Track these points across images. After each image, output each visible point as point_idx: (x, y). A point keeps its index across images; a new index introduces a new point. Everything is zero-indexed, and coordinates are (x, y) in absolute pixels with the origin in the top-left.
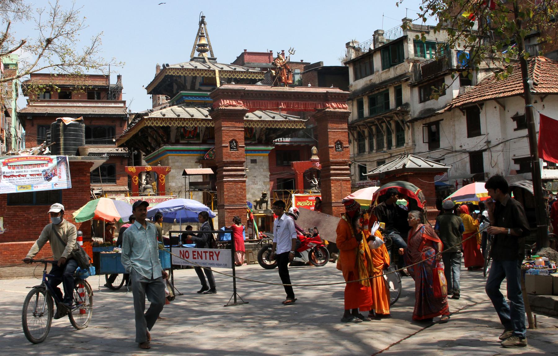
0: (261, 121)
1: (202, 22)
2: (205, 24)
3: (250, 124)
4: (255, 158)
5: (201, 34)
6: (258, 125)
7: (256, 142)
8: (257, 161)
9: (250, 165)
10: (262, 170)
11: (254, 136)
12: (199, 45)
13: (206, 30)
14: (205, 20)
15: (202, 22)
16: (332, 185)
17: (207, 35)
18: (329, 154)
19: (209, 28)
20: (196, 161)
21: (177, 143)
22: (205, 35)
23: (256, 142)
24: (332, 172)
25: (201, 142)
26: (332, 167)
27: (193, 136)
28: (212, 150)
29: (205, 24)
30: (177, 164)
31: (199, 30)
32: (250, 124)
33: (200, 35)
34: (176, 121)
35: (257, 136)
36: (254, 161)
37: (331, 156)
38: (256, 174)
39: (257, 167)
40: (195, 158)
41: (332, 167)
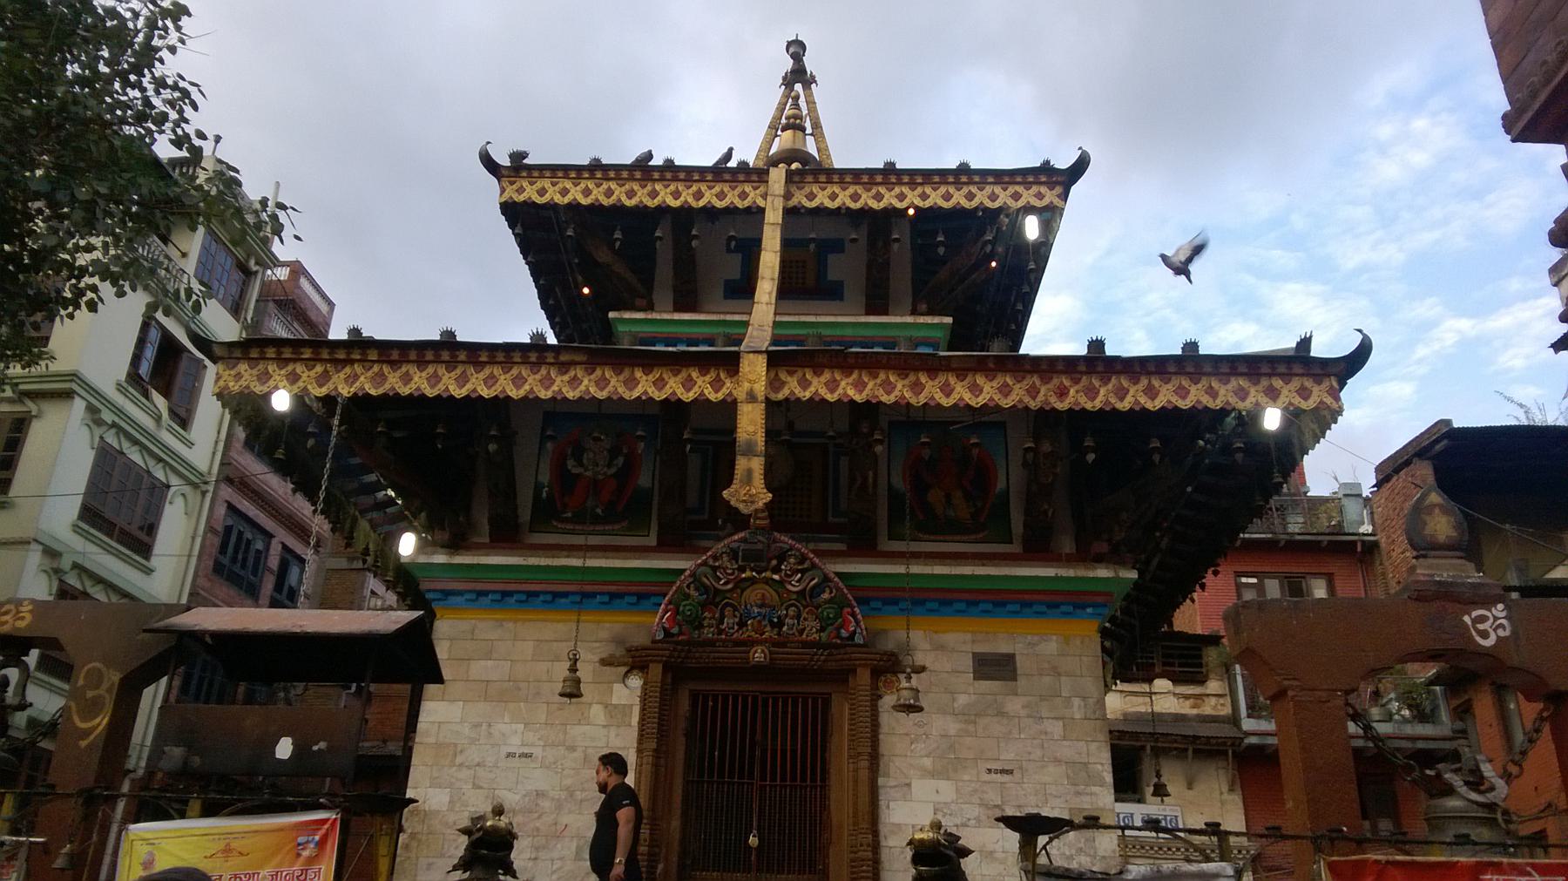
1: (798, 76)
4: (1004, 648)
9: (969, 692)
10: (1056, 728)
13: (811, 103)
14: (810, 63)
15: (798, 76)
19: (826, 98)
20: (605, 651)
22: (808, 125)
23: (1015, 548)
25: (652, 540)
28: (693, 575)
30: (479, 669)
31: (781, 108)
36: (996, 667)
38: (1009, 755)
39: (1014, 705)
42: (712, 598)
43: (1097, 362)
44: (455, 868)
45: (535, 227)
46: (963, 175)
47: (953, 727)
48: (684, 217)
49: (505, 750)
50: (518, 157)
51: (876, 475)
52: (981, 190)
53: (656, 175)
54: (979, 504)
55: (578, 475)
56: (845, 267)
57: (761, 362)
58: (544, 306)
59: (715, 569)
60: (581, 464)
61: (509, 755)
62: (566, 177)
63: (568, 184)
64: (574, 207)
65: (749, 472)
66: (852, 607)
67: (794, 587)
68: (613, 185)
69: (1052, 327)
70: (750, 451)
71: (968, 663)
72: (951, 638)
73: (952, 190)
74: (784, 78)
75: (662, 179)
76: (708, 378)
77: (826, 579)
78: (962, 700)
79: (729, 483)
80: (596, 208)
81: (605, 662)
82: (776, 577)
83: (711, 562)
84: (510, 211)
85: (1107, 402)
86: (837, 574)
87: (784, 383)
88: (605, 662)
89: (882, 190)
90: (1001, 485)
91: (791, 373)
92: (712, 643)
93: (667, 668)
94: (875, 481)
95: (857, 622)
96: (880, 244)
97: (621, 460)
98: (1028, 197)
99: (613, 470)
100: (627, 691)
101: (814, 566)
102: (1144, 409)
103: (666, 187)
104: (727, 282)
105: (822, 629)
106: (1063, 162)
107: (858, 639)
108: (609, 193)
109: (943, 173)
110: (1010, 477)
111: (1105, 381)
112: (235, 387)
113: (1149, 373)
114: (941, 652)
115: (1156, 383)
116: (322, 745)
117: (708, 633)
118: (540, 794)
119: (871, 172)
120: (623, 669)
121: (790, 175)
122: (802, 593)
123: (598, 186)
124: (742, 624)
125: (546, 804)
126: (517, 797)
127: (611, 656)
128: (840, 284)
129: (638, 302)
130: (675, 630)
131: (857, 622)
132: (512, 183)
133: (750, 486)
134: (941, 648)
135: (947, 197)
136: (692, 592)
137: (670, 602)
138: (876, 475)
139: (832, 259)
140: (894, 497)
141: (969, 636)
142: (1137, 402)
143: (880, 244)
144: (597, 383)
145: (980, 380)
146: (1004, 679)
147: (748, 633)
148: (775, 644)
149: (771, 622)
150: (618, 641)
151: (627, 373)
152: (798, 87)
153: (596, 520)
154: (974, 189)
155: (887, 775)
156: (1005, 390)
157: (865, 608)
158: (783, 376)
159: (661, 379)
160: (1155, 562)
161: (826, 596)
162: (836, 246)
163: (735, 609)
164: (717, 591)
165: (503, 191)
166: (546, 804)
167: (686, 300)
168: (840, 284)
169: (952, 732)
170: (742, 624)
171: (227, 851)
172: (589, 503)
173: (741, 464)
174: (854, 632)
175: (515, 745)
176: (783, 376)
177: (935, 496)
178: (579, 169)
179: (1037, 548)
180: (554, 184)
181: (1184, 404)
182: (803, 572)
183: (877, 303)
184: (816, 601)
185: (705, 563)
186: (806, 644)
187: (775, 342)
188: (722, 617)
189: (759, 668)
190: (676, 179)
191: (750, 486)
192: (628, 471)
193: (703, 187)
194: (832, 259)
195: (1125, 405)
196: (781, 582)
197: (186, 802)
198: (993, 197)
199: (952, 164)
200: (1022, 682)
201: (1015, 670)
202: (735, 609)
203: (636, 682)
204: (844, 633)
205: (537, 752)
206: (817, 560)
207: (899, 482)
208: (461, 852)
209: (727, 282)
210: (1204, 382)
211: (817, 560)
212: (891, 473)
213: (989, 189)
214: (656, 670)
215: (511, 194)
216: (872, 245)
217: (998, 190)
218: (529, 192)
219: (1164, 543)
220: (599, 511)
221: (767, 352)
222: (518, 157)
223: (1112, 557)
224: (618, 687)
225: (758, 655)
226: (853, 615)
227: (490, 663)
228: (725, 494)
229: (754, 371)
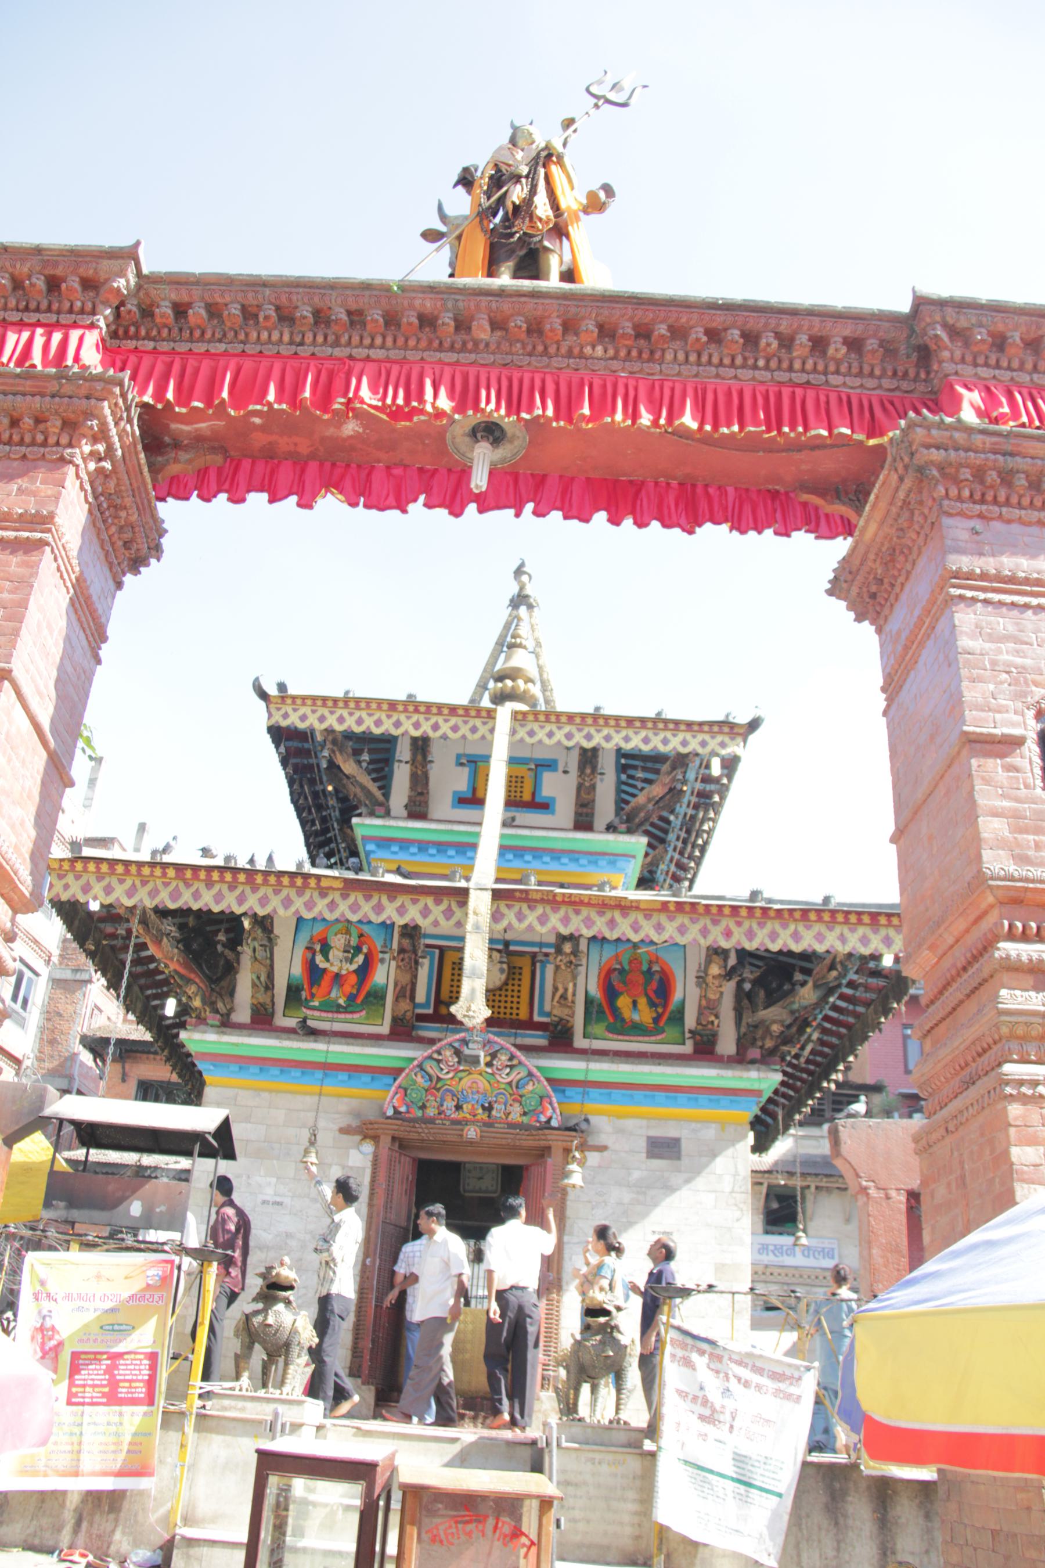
0: (680, 906)
1: (520, 600)
2: (530, 607)
3: (612, 924)
4: (670, 1131)
5: (513, 637)
6: (659, 928)
7: (688, 1048)
8: (684, 1145)
9: (644, 1168)
11: (678, 1017)
12: (500, 678)
16: (1021, 1155)
17: (538, 644)
18: (971, 813)
21: (262, 1020)
24: (1018, 999)
25: (385, 1029)
26: (1009, 949)
27: (351, 998)
28: (420, 1067)
29: (530, 607)
31: (507, 626)
32: (612, 924)
33: (508, 643)
34: (209, 884)
35: (690, 1020)
36: (663, 1148)
37: (991, 827)
40: (344, 1105)
41: (1009, 949)
42: (435, 1085)
43: (758, 911)
44: (254, 1300)
45: (294, 746)
46: (659, 723)
47: (627, 1196)
48: (421, 746)
49: (261, 1198)
50: (282, 687)
51: (575, 985)
52: (674, 735)
53: (401, 708)
54: (660, 1010)
55: (325, 970)
56: (560, 788)
57: (488, 896)
58: (294, 801)
59: (439, 1061)
60: (328, 960)
61: (264, 1202)
62: (324, 705)
63: (325, 712)
64: (329, 731)
65: (473, 991)
66: (550, 1097)
67: (504, 1077)
68: (364, 714)
69: (726, 870)
70: (474, 975)
71: (642, 1144)
72: (630, 1123)
73: (650, 734)
74: (512, 601)
75: (406, 710)
76: (444, 906)
77: (530, 1074)
78: (636, 1175)
79: (455, 998)
80: (349, 735)
81: (345, 1131)
82: (489, 1070)
83: (435, 1056)
84: (278, 734)
85: (762, 944)
86: (537, 1067)
87: (503, 915)
88: (345, 1131)
89: (592, 730)
90: (677, 996)
91: (509, 907)
92: (431, 1121)
93: (394, 1139)
94: (574, 995)
95: (554, 1109)
96: (588, 771)
97: (360, 959)
98: (713, 744)
99: (354, 967)
100: (361, 1156)
101: (520, 1063)
102: (790, 954)
103: (408, 718)
104: (455, 793)
105: (525, 1114)
106: (742, 718)
107: (554, 1123)
108: (360, 722)
109: (643, 721)
110: (686, 992)
111: (762, 925)
112: (64, 897)
113: (796, 920)
114: (620, 1132)
115: (801, 928)
116: (163, 1208)
117: (431, 1112)
118: (289, 1235)
119: (583, 716)
120: (358, 1138)
121: (515, 715)
122: (510, 1084)
123: (351, 714)
124: (458, 1107)
125: (293, 1243)
126: (270, 1237)
127: (349, 1126)
128: (553, 799)
129: (380, 811)
130: (403, 1109)
131: (554, 1109)
132: (278, 709)
133: (472, 1006)
134: (620, 1131)
135: (646, 741)
136: (419, 1079)
137: (400, 1087)
138: (575, 985)
139: (547, 777)
140: (589, 1002)
141: (644, 1122)
142: (785, 944)
143: (588, 771)
144: (351, 908)
145: (663, 918)
146: (670, 1158)
147: (464, 1114)
148: (485, 1124)
149: (483, 1106)
150: (356, 1114)
151: (374, 901)
152: (523, 610)
153: (339, 1009)
154: (669, 734)
155: (571, 1234)
156: (682, 930)
157: (561, 1095)
158: (503, 909)
159: (403, 906)
160: (809, 1048)
161: (530, 1087)
162: (550, 765)
163: (454, 1095)
164: (439, 1079)
165: (270, 715)
166: (293, 1243)
167: (417, 810)
168: (553, 799)
169: (626, 1200)
170: (458, 1107)
171: (98, 1277)
172: (333, 995)
173: (466, 986)
174: (550, 1118)
175: (269, 1193)
176: (503, 909)
177: (623, 1002)
178: (335, 701)
179: (705, 1049)
180: (314, 712)
181: (820, 948)
182: (512, 1067)
183: (583, 822)
184: (521, 1091)
185: (430, 1057)
186: (512, 1125)
187: (498, 880)
188: (443, 1100)
189: (471, 1143)
190: (416, 711)
191: (472, 1006)
192: (365, 971)
193: (440, 720)
194: (547, 777)
195: (775, 947)
196: (493, 1074)
197: (68, 1242)
198: (684, 743)
199: (652, 714)
200: (685, 1161)
201: (679, 1152)
202: (454, 1095)
203: (368, 1148)
204: (543, 1119)
205: (287, 1201)
206: (523, 1058)
207: (594, 990)
208: (257, 1290)
209: (455, 793)
210: (838, 930)
211: (523, 1058)
212: (588, 983)
213: (681, 736)
214: (386, 1141)
215: (278, 719)
216: (581, 769)
217: (688, 736)
218: (294, 720)
219: (815, 1036)
220: (341, 1001)
221: (494, 891)
222: (282, 687)
223: (766, 1059)
224: (353, 1153)
225: (472, 1133)
226: (551, 1104)
227: (249, 1126)
228: (453, 1009)
229: (480, 903)
